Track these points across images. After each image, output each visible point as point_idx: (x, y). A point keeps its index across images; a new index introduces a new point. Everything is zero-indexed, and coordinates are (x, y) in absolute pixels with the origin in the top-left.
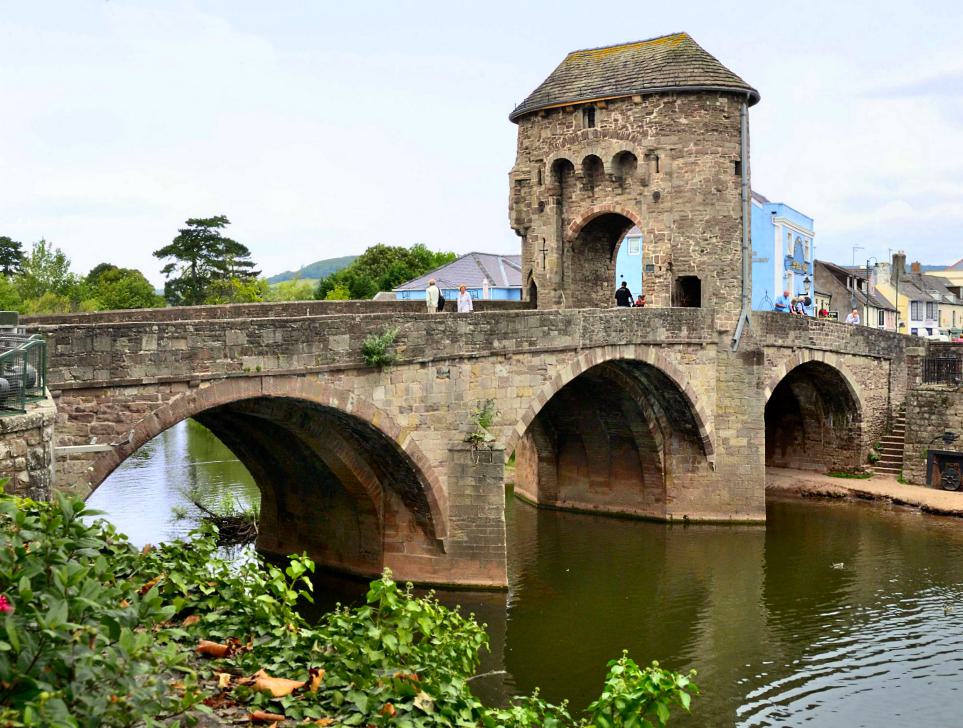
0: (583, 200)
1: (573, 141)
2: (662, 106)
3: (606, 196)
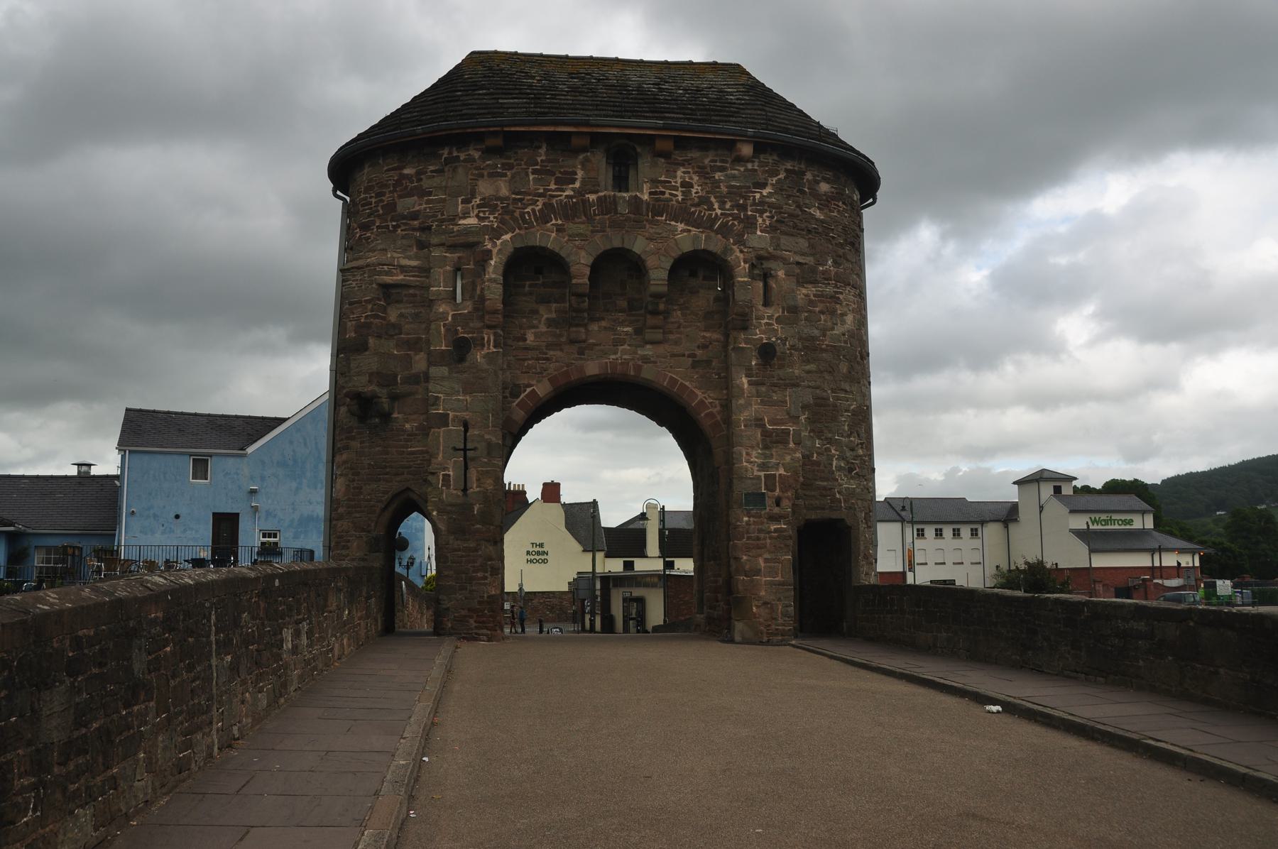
0: (550, 346)
1: (571, 211)
2: (782, 176)
3: (618, 342)
